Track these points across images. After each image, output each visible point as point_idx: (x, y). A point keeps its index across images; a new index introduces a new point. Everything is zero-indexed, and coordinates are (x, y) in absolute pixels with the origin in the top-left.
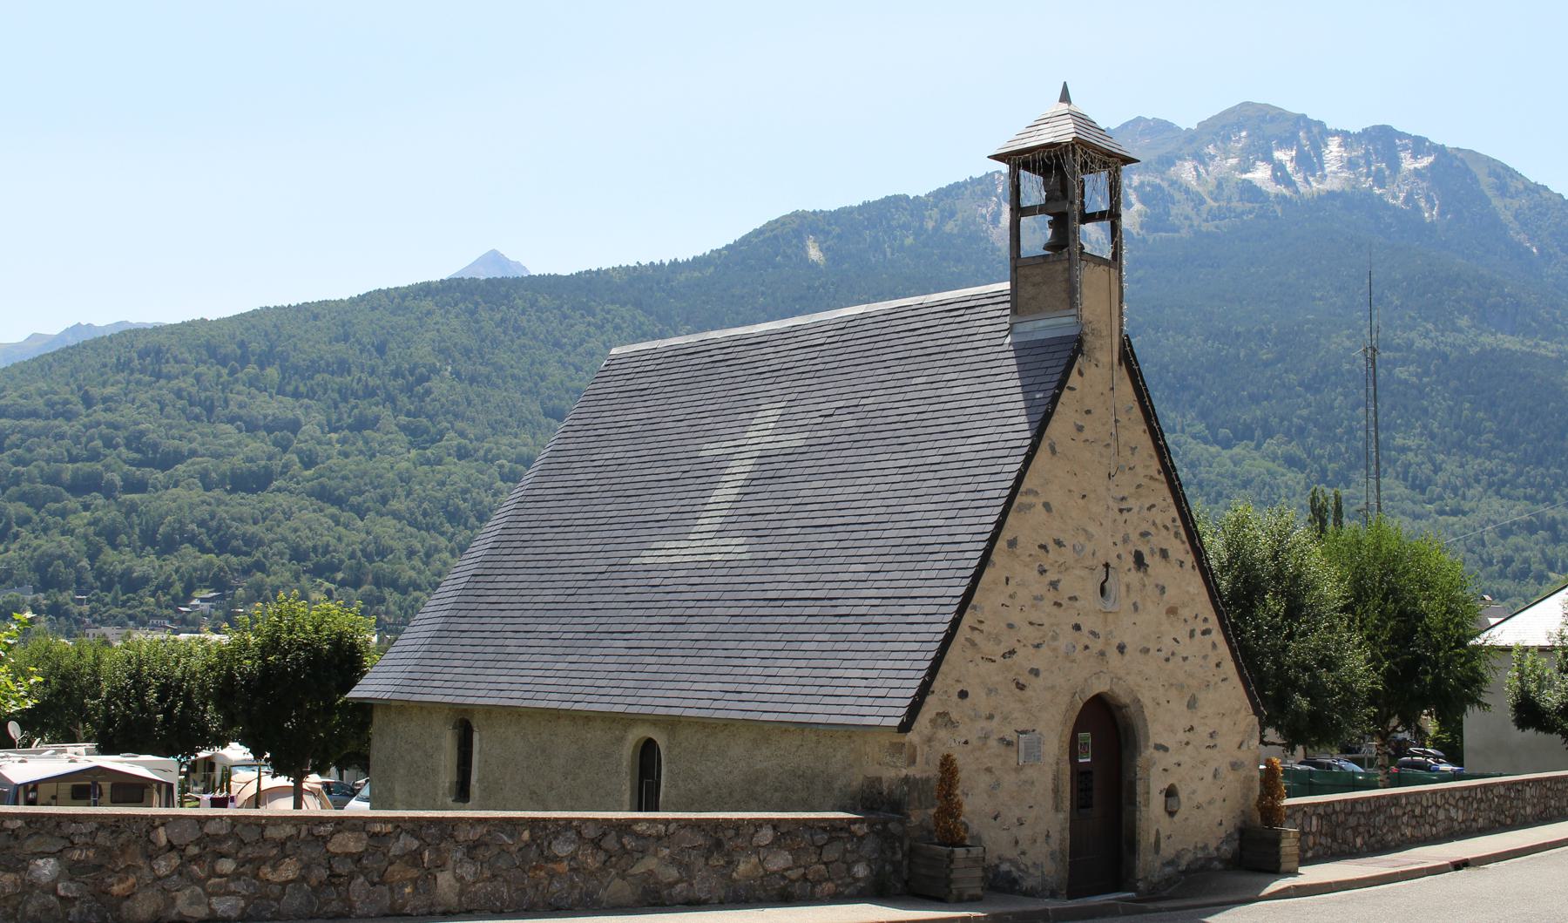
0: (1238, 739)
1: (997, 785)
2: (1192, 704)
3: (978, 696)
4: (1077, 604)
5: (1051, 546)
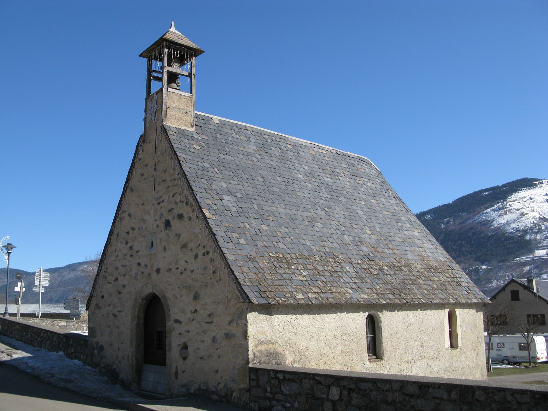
0: (229, 318)
1: (111, 333)
2: (196, 297)
3: (106, 296)
4: (139, 254)
5: (130, 231)
